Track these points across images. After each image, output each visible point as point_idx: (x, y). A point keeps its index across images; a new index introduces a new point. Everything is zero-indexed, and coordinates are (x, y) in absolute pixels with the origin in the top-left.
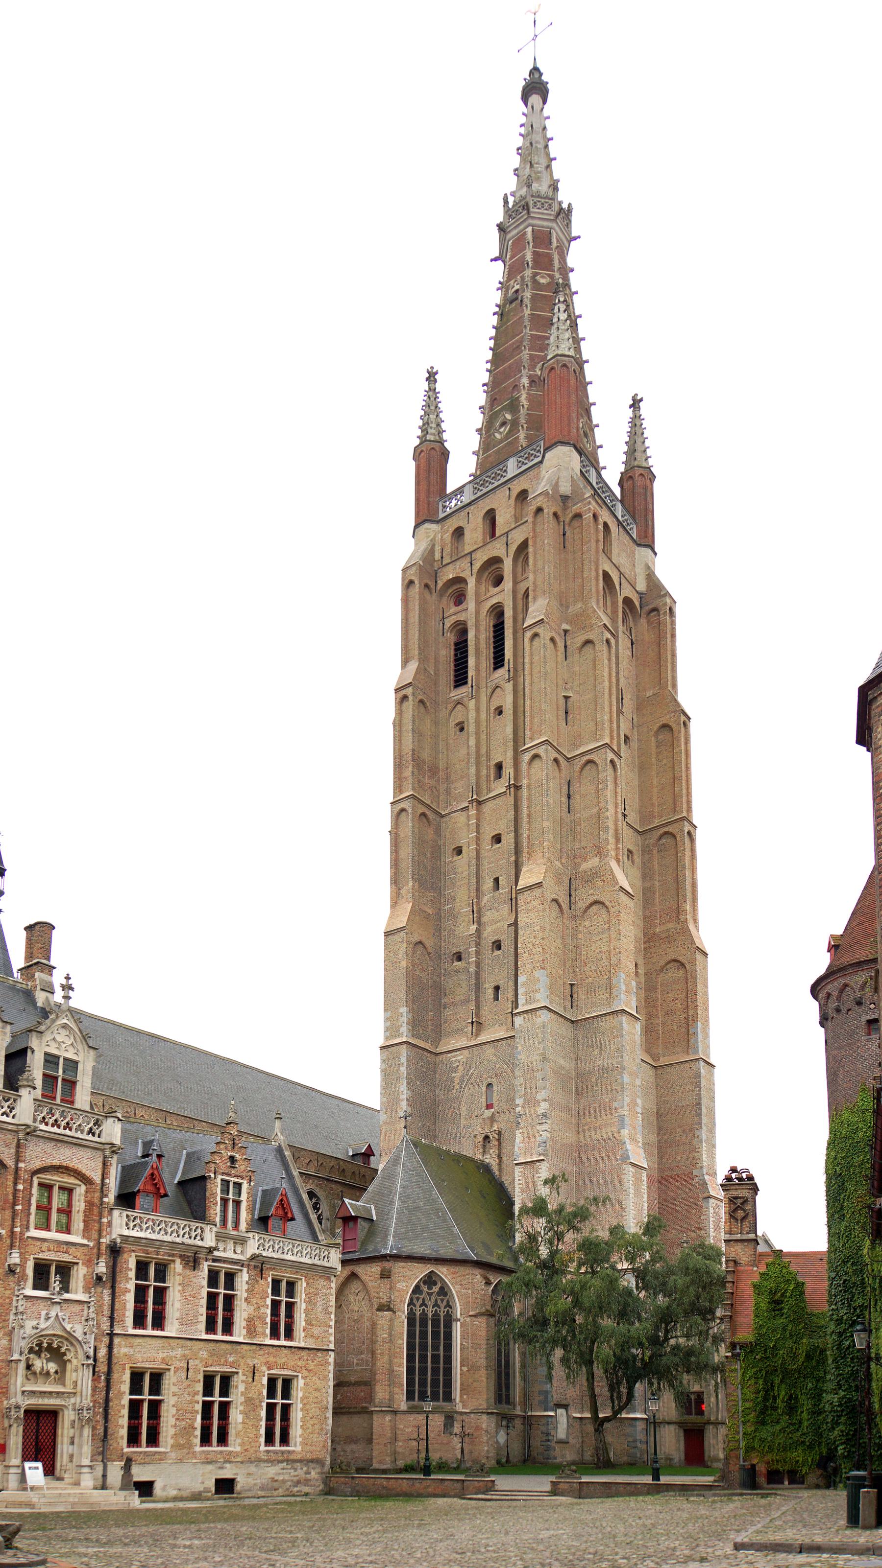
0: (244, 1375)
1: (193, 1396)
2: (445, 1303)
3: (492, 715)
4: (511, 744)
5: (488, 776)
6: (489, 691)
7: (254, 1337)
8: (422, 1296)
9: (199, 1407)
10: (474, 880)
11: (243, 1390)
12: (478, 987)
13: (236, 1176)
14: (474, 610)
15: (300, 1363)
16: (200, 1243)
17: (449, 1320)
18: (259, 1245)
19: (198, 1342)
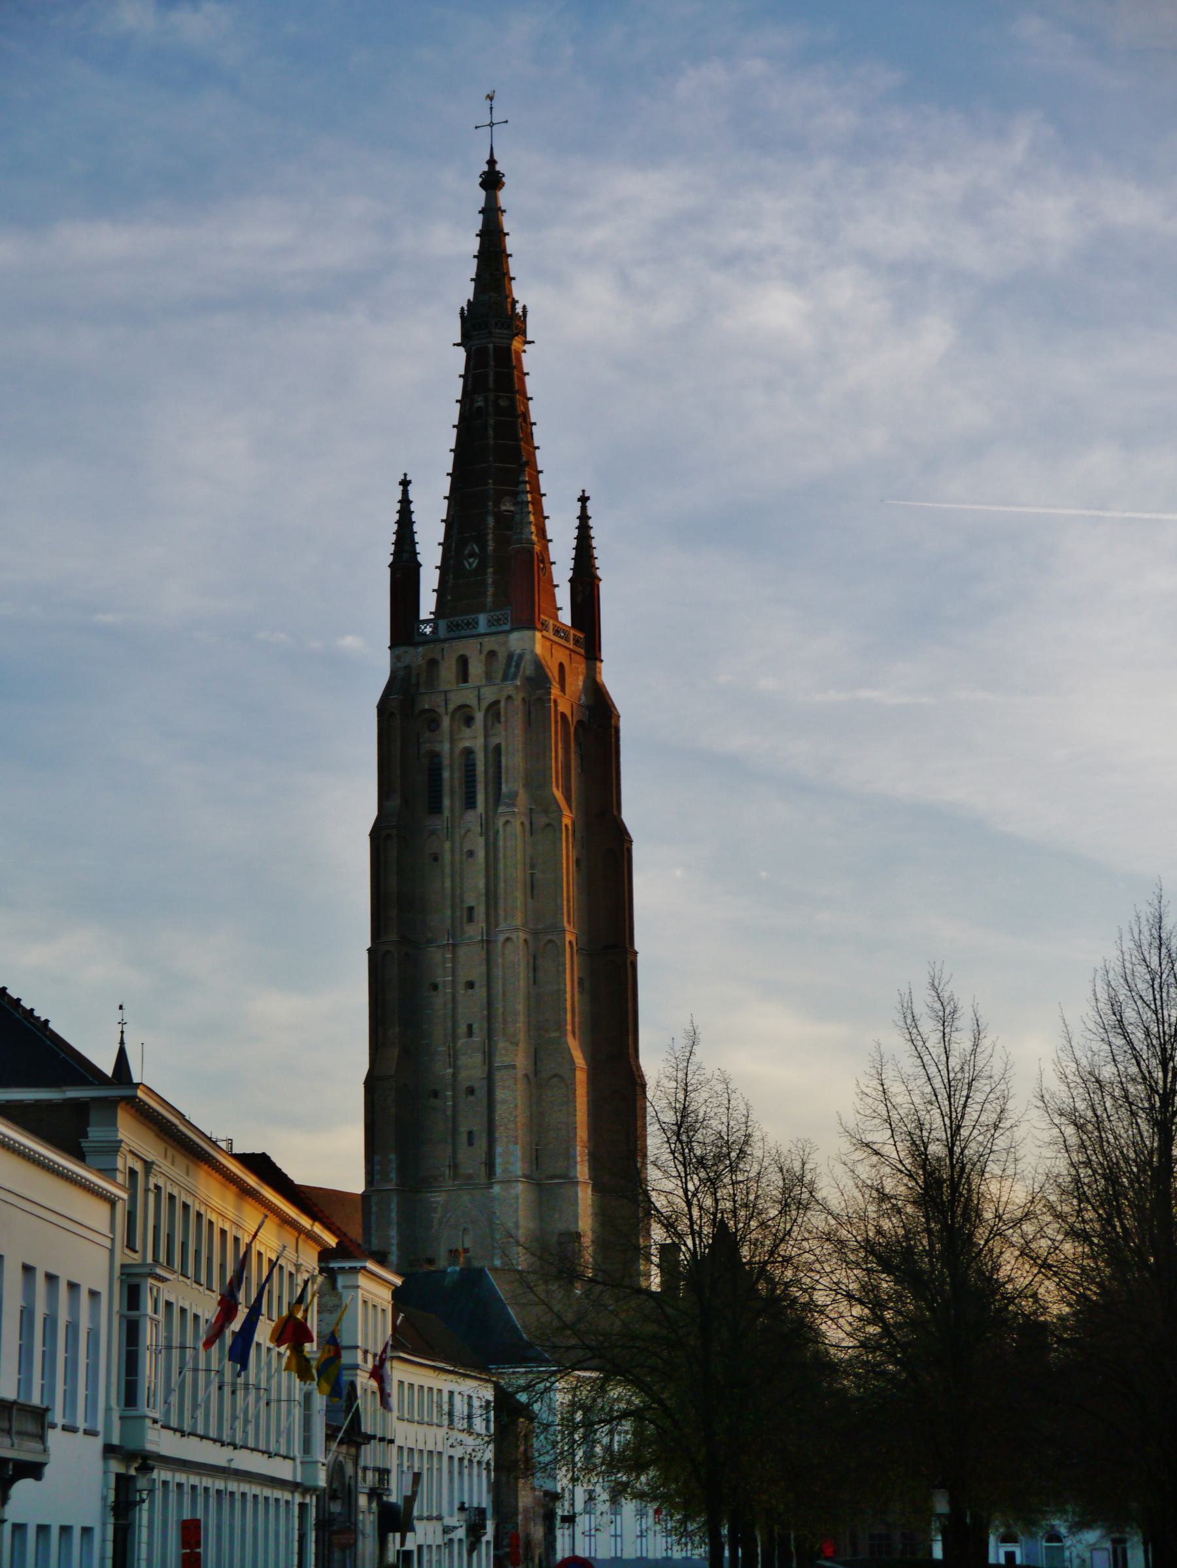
3: (464, 857)
6: (463, 831)
10: (450, 1024)
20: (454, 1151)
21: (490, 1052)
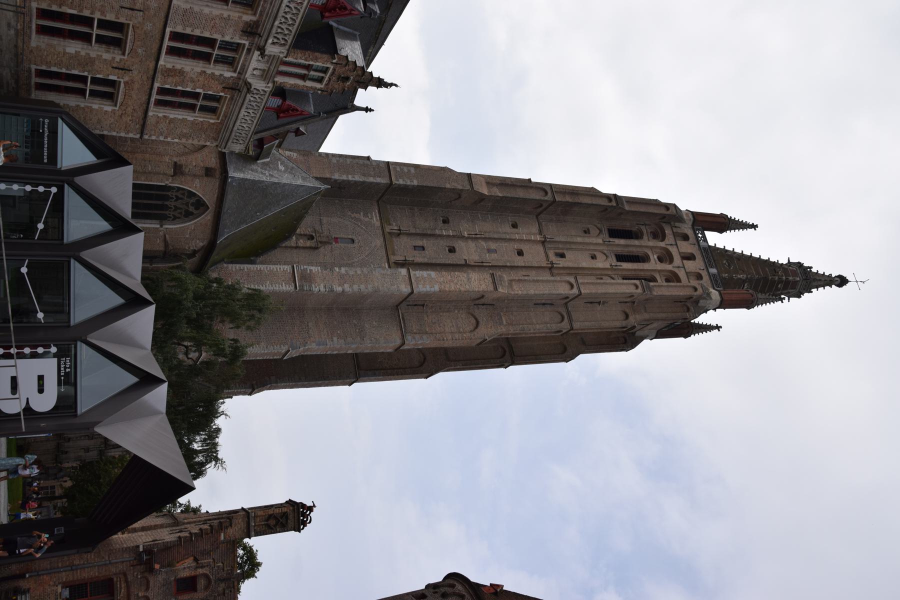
0: (121, 60)
1: (99, 10)
2: (178, 215)
4: (576, 266)
5: (558, 248)
6: (605, 252)
7: (163, 75)
8: (186, 199)
9: (86, 13)
11: (104, 57)
12: (424, 235)
13: (330, 79)
14: (648, 245)
15: (130, 110)
16: (270, 41)
17: (162, 218)
18: (258, 90)
19: (162, 24)
20: (410, 235)
21: (483, 266)
